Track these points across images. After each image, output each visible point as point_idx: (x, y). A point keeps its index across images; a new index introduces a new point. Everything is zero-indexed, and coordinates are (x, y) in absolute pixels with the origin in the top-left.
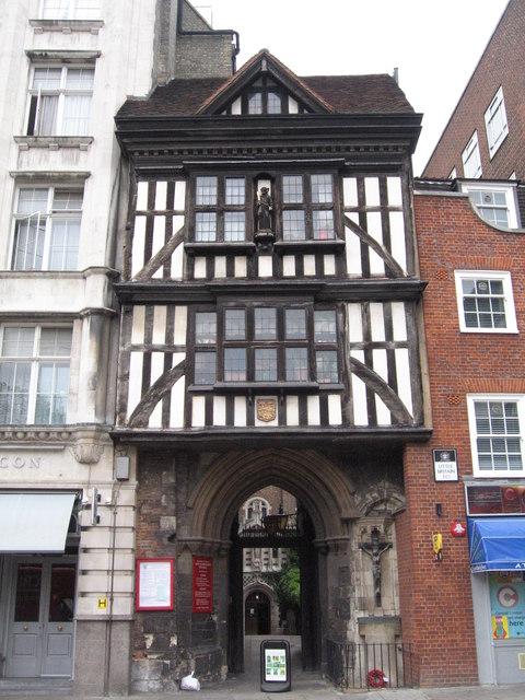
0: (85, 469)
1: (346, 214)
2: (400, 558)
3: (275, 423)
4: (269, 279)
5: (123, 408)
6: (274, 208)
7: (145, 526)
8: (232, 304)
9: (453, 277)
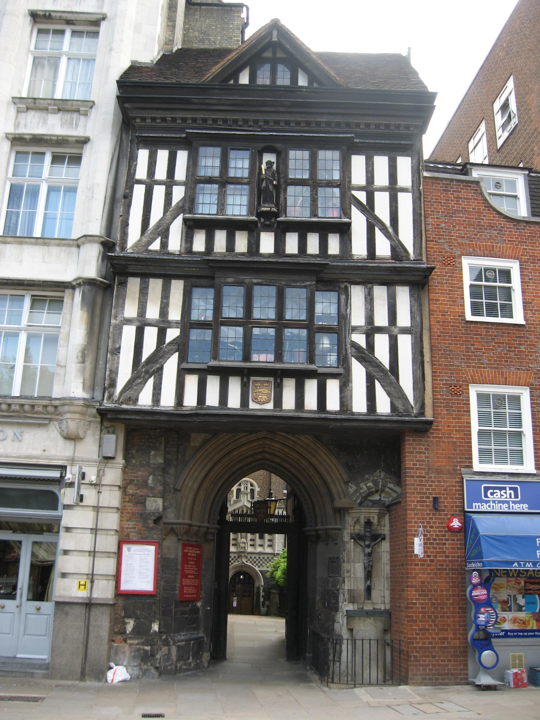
0: (69, 445)
1: (354, 192)
2: (393, 552)
3: (270, 406)
4: (270, 255)
5: (113, 384)
6: (279, 182)
7: (130, 507)
8: (230, 280)
9: (461, 263)
